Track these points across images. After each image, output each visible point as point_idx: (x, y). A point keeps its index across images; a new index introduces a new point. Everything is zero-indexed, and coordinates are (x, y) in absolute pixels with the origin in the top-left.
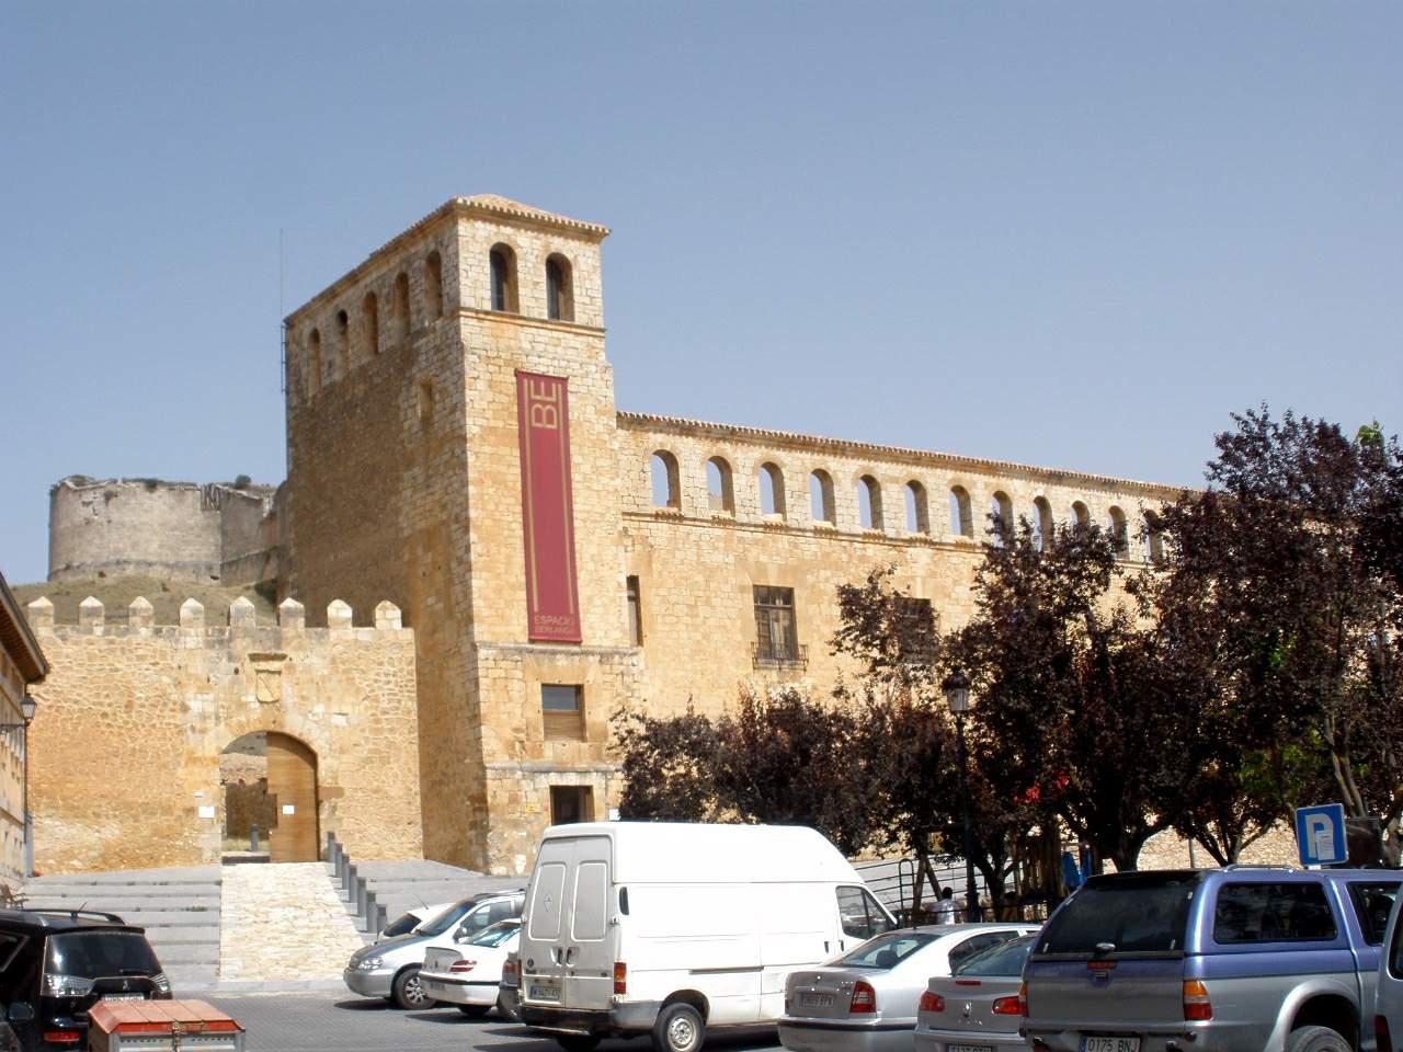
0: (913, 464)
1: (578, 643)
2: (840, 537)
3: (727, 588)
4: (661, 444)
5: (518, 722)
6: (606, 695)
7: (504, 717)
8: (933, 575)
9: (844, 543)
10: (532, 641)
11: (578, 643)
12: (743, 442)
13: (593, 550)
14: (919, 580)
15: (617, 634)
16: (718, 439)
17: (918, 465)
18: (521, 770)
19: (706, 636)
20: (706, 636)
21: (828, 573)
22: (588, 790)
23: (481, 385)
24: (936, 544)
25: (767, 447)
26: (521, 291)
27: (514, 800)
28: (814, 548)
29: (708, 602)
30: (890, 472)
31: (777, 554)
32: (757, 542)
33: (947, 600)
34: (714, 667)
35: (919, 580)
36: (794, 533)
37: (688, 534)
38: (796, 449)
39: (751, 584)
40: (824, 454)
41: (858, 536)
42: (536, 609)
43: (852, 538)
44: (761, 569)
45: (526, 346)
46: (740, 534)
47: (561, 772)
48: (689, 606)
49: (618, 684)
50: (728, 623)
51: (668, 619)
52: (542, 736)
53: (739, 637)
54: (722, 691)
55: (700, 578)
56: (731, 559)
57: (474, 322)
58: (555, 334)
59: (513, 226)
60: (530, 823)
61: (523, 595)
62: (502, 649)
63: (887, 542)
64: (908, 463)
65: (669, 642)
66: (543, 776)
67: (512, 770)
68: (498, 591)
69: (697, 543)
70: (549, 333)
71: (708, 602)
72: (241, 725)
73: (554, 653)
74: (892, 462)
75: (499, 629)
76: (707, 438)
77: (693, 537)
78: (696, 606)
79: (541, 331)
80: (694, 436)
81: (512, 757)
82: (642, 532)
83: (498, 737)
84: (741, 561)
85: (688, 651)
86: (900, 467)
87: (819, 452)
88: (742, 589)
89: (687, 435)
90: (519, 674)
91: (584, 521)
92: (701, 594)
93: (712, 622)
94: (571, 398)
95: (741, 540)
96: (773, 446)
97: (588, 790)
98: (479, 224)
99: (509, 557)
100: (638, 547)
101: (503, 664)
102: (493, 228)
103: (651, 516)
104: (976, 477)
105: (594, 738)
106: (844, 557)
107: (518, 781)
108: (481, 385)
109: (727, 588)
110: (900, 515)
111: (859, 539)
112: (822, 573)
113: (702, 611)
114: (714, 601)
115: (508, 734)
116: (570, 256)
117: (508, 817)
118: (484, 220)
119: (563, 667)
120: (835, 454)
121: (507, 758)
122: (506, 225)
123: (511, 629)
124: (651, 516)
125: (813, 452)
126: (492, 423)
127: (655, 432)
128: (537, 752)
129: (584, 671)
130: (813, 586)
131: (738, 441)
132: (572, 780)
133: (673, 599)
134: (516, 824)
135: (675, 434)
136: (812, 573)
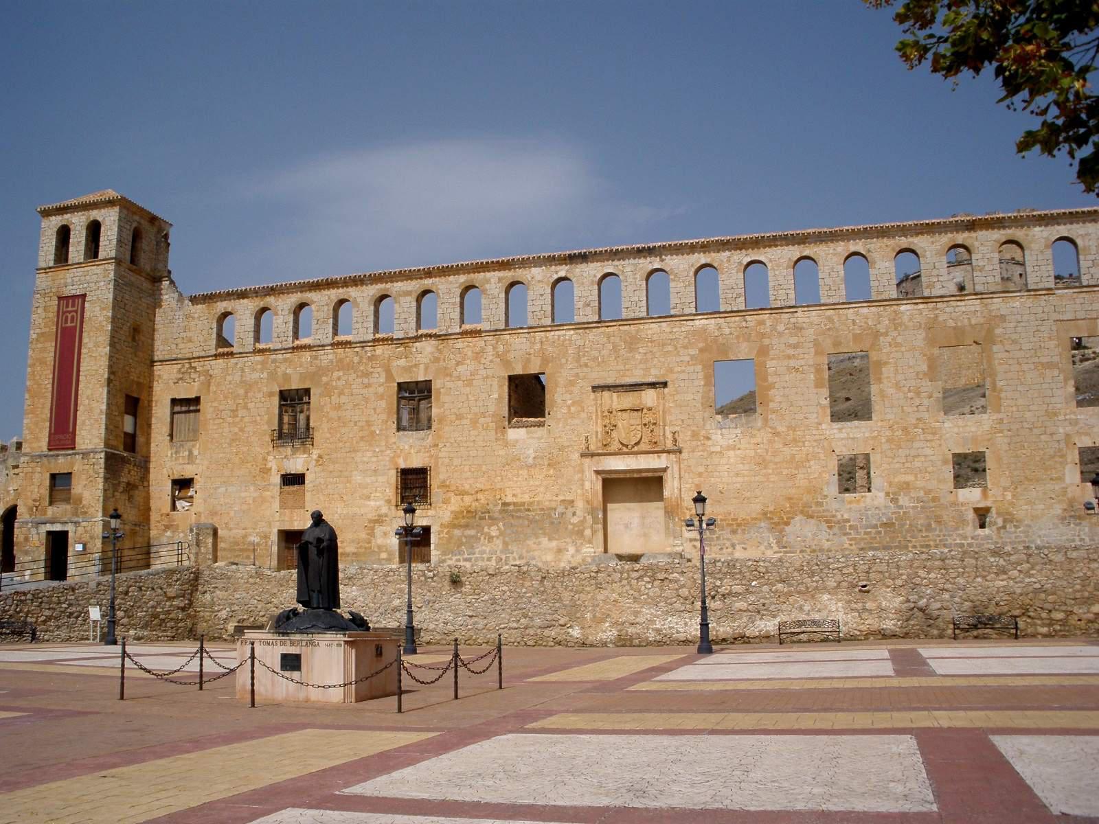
0: (426, 278)
1: (74, 448)
2: (353, 346)
3: (260, 395)
4: (225, 308)
5: (36, 496)
6: (84, 477)
7: (29, 494)
8: (437, 360)
9: (356, 350)
10: (50, 450)
11: (74, 448)
12: (283, 293)
13: (89, 392)
14: (422, 367)
15: (97, 441)
16: (265, 295)
17: (430, 277)
18: (31, 522)
19: (241, 430)
20: (241, 430)
21: (341, 373)
22: (66, 533)
23: (40, 310)
24: (440, 336)
25: (301, 292)
26: (71, 249)
27: (27, 539)
28: (330, 357)
29: (246, 407)
30: (404, 288)
31: (301, 366)
32: (285, 360)
33: (448, 378)
34: (245, 449)
35: (422, 367)
36: (315, 349)
37: (237, 363)
38: (324, 289)
39: (278, 390)
40: (347, 287)
41: (369, 342)
42: (53, 431)
43: (362, 345)
44: (287, 377)
45: (69, 280)
46: (273, 357)
47: (52, 523)
48: (232, 411)
49: (91, 472)
50: (258, 418)
51: (217, 421)
52: (47, 503)
53: (265, 427)
54: (249, 465)
55: (241, 392)
56: (265, 375)
57: (44, 275)
58: (86, 269)
59: (70, 213)
60: (34, 552)
61: (48, 424)
62: (32, 456)
63: (395, 342)
64: (421, 278)
65: (216, 435)
66: (43, 526)
67: (27, 523)
68: (36, 424)
69: (242, 369)
70: (82, 269)
71: (246, 407)
72: (7, 502)
73: (58, 456)
74: (407, 280)
75: (35, 445)
76: (257, 297)
77: (239, 366)
78: (237, 410)
79: (79, 270)
80: (247, 298)
81: (31, 516)
82: (205, 368)
83: (25, 505)
84: (272, 376)
85: (228, 441)
86: (414, 283)
87: (343, 287)
88: (271, 394)
89: (243, 298)
90: (39, 469)
91: (86, 376)
92: (241, 401)
93: (246, 419)
94: (87, 305)
95: (274, 361)
96: (306, 291)
97: (66, 533)
98: (53, 218)
99: (44, 404)
100: (202, 378)
101: (32, 465)
102: (59, 218)
103: (212, 356)
104: (488, 275)
105: (75, 503)
106: (356, 360)
107: (29, 529)
108: (40, 310)
109: (260, 395)
110: (409, 320)
111: (370, 344)
112: (336, 374)
113: (241, 413)
114: (250, 405)
115: (30, 503)
116: (100, 219)
117: (23, 549)
118: (55, 215)
119: (61, 464)
120: (356, 285)
121: (28, 516)
122: (66, 213)
123: (40, 444)
124: (212, 356)
125: (338, 288)
126: (43, 331)
127: (222, 301)
128: (44, 512)
129: (72, 464)
130: (327, 384)
131: (279, 294)
132: (57, 528)
133: (221, 407)
134: (26, 553)
135: (234, 299)
136: (327, 375)
